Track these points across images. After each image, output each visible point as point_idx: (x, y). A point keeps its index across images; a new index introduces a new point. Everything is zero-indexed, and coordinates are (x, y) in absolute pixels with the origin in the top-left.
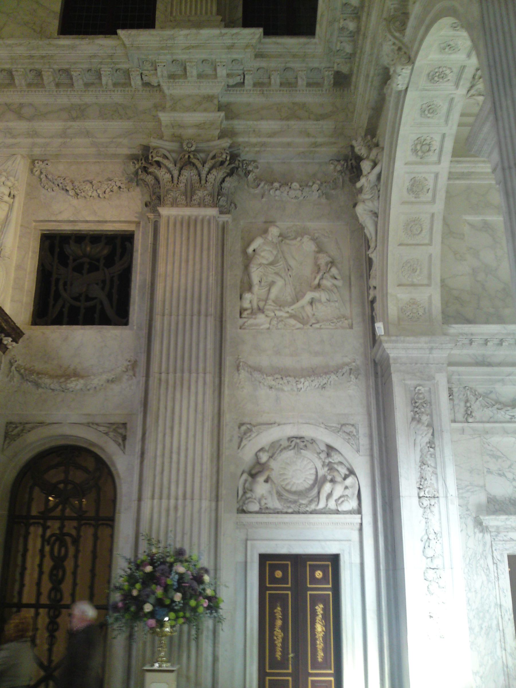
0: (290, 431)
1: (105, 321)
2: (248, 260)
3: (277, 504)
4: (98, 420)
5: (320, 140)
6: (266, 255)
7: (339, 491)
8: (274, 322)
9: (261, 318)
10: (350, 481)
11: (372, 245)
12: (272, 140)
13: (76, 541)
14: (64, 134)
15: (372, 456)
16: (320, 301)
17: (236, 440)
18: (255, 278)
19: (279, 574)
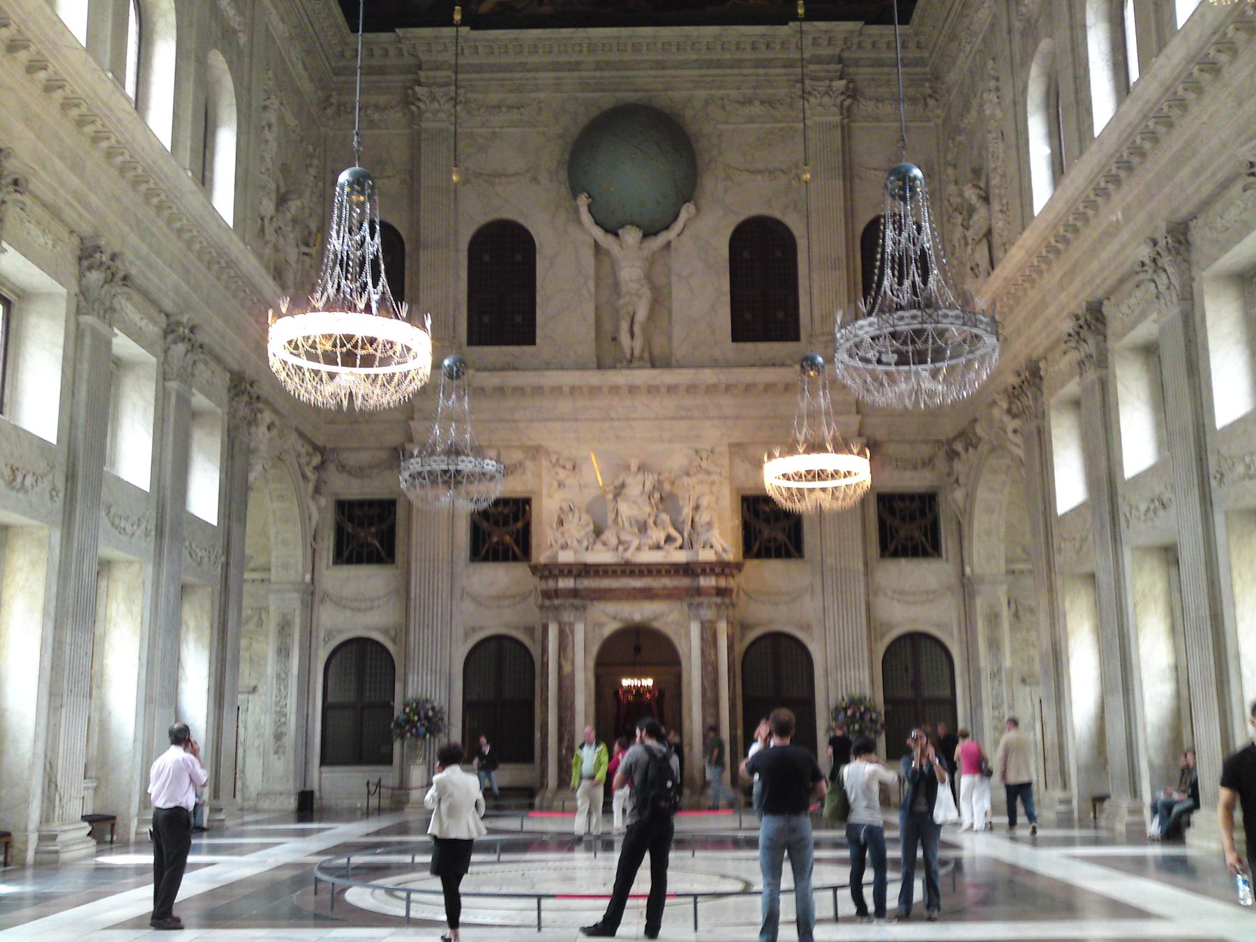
1: (788, 555)
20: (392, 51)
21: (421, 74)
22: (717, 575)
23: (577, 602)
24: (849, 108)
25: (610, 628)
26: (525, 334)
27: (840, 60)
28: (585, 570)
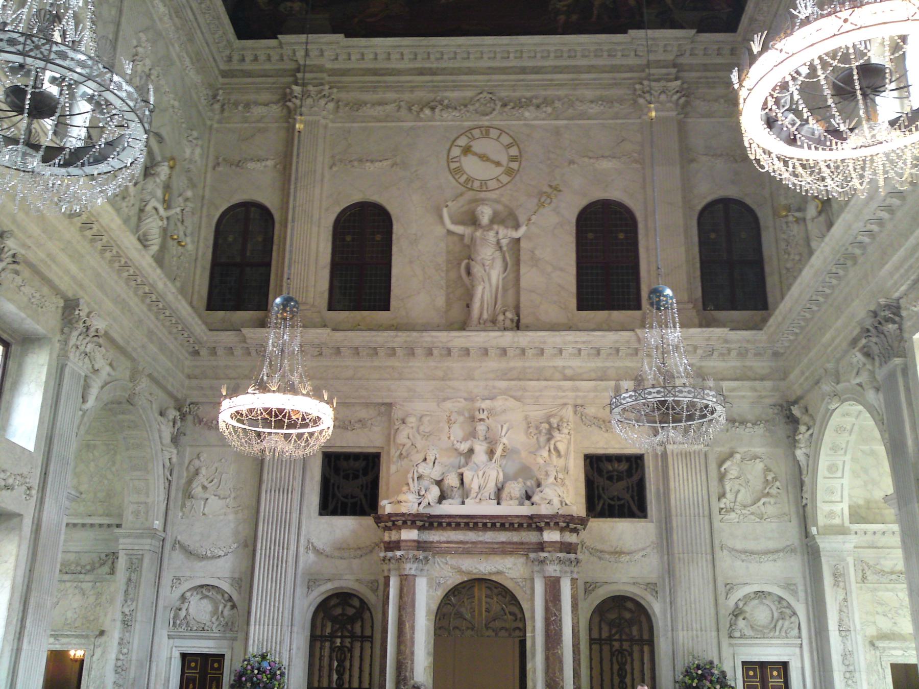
0: (756, 588)
1: (632, 515)
2: (722, 477)
3: (752, 633)
4: (640, 581)
5: (764, 394)
6: (733, 473)
7: (787, 623)
8: (741, 517)
9: (733, 515)
10: (793, 618)
11: (804, 472)
12: (732, 394)
13: (631, 655)
14: (595, 389)
15: (807, 603)
16: (770, 503)
17: (724, 594)
18: (728, 488)
19: (751, 673)
20: (275, 57)
21: (299, 75)
22: (562, 530)
23: (421, 555)
24: (684, 106)
25: (455, 579)
26: (384, 304)
27: (675, 66)
28: (429, 522)
